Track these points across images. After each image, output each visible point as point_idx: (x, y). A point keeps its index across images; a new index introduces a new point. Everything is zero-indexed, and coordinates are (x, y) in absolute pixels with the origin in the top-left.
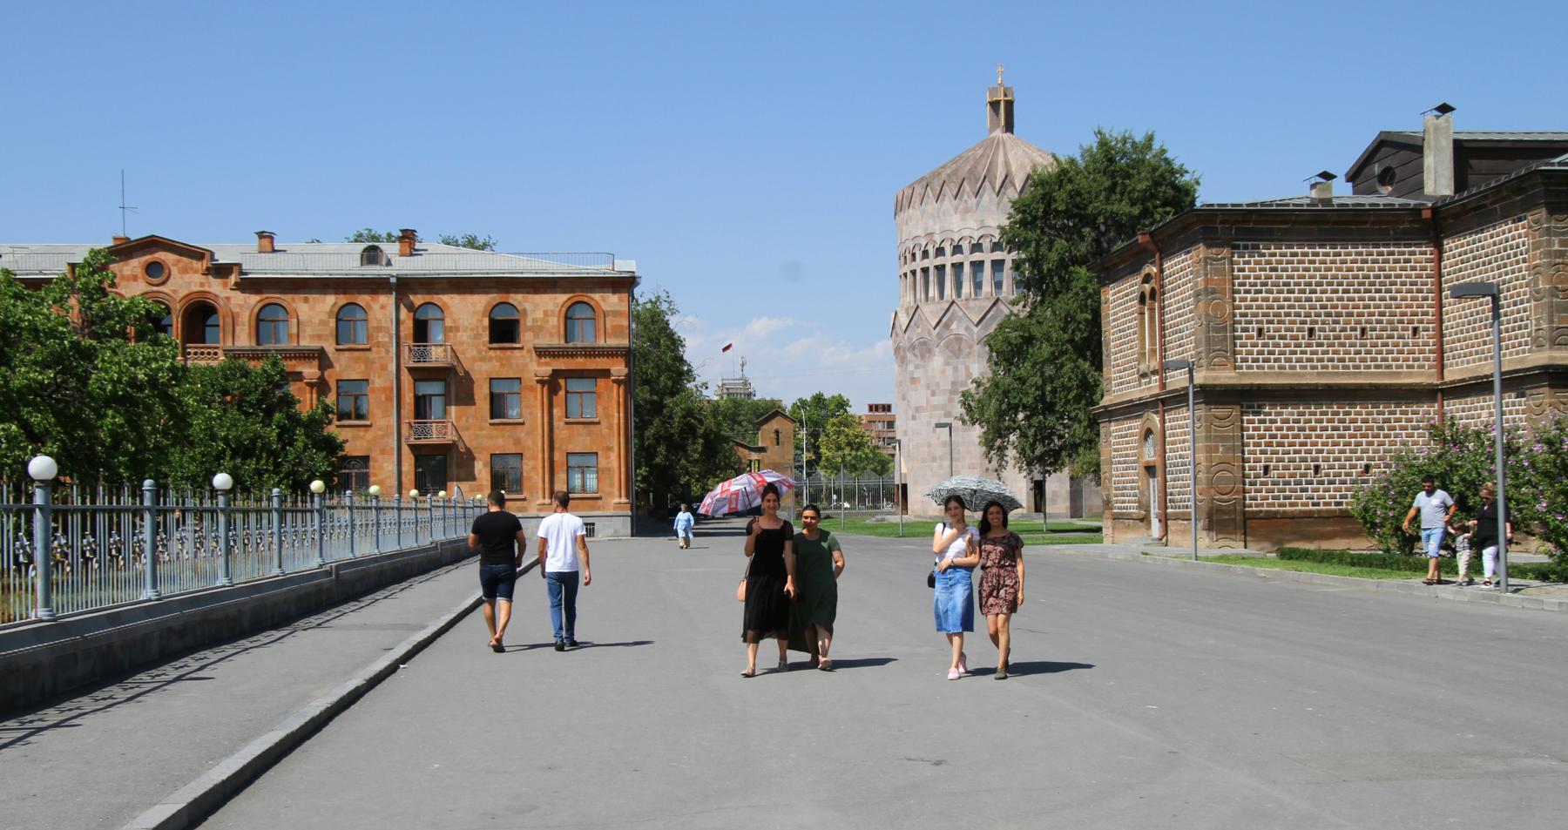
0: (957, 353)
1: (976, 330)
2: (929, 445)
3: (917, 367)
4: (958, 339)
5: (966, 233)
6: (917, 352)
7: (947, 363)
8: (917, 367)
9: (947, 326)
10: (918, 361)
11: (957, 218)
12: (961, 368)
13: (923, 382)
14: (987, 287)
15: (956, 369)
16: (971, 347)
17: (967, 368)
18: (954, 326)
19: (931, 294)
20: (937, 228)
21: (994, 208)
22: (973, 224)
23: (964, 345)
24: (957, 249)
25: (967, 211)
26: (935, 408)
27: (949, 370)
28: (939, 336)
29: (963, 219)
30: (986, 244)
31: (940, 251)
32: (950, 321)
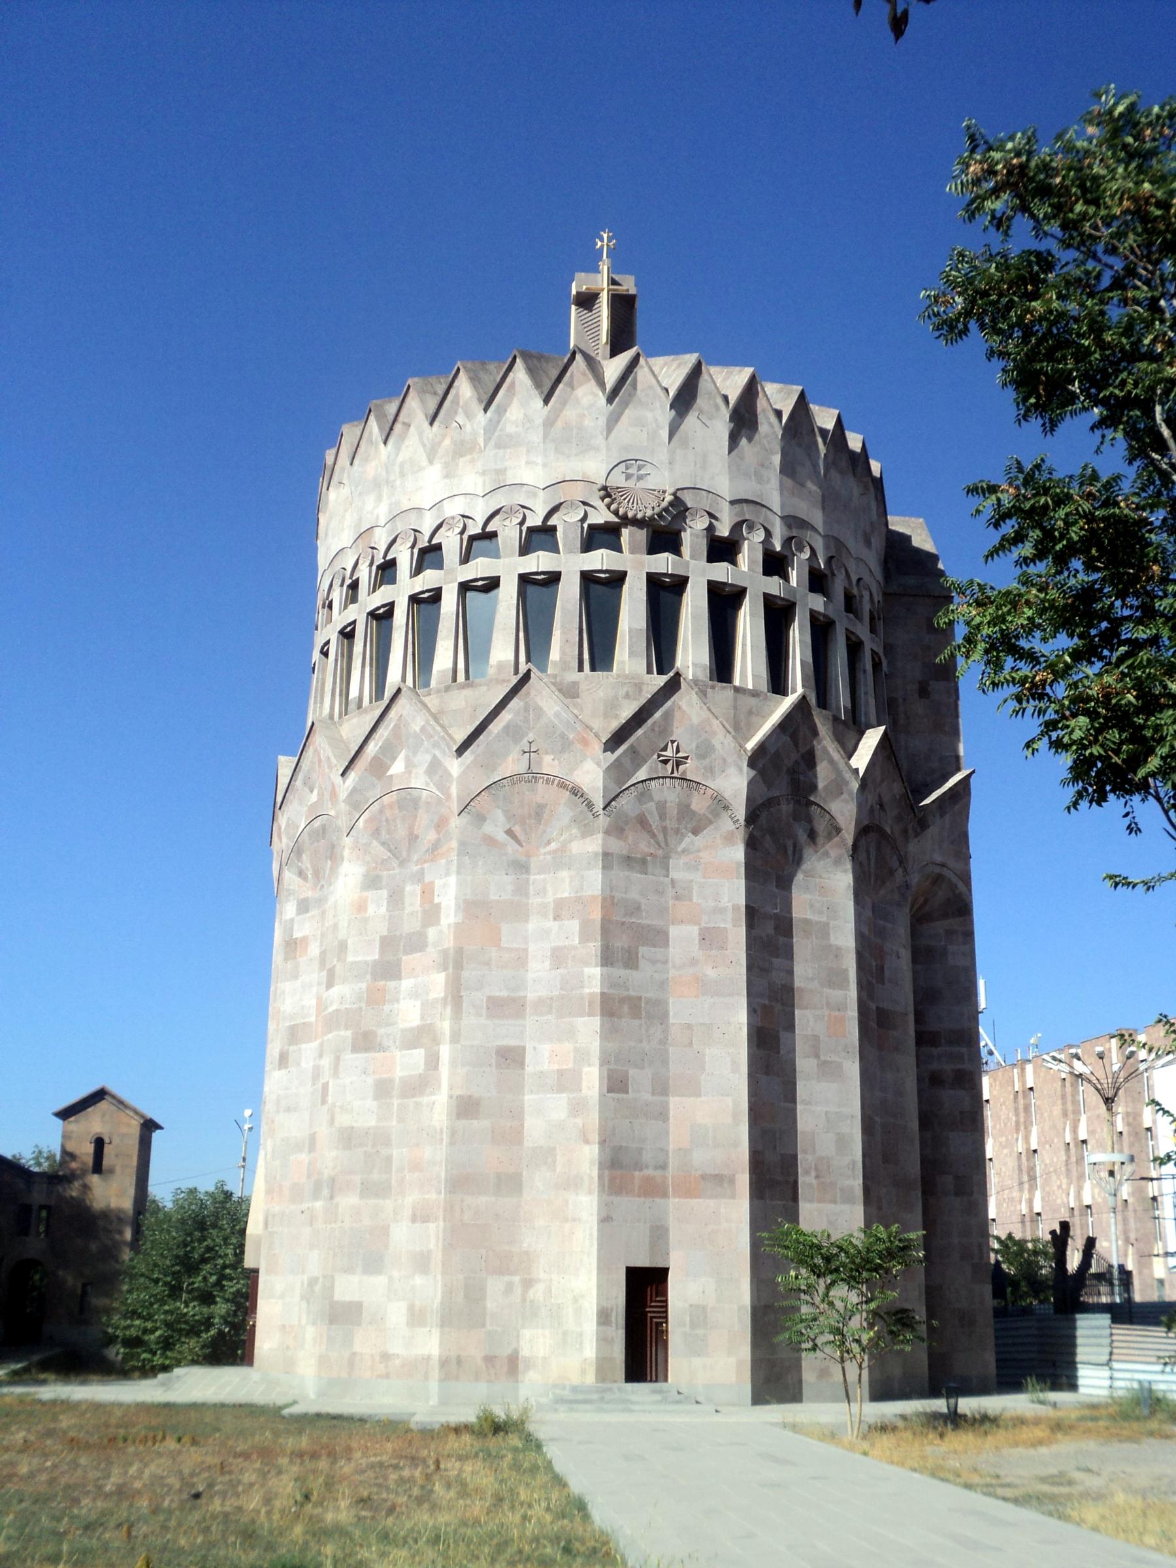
0: (399, 852)
1: (455, 766)
2: (312, 1142)
3: (304, 907)
4: (409, 801)
5: (453, 509)
6: (306, 862)
7: (371, 882)
8: (304, 907)
9: (379, 767)
10: (307, 891)
11: (434, 472)
12: (412, 892)
13: (314, 950)
14: (503, 649)
15: (396, 898)
16: (441, 824)
17: (428, 892)
18: (397, 767)
19: (354, 693)
20: (382, 513)
21: (536, 437)
22: (472, 480)
23: (424, 819)
24: (429, 555)
25: (462, 449)
26: (333, 1021)
27: (378, 906)
28: (356, 802)
29: (449, 474)
30: (509, 533)
31: (387, 570)
32: (389, 751)
